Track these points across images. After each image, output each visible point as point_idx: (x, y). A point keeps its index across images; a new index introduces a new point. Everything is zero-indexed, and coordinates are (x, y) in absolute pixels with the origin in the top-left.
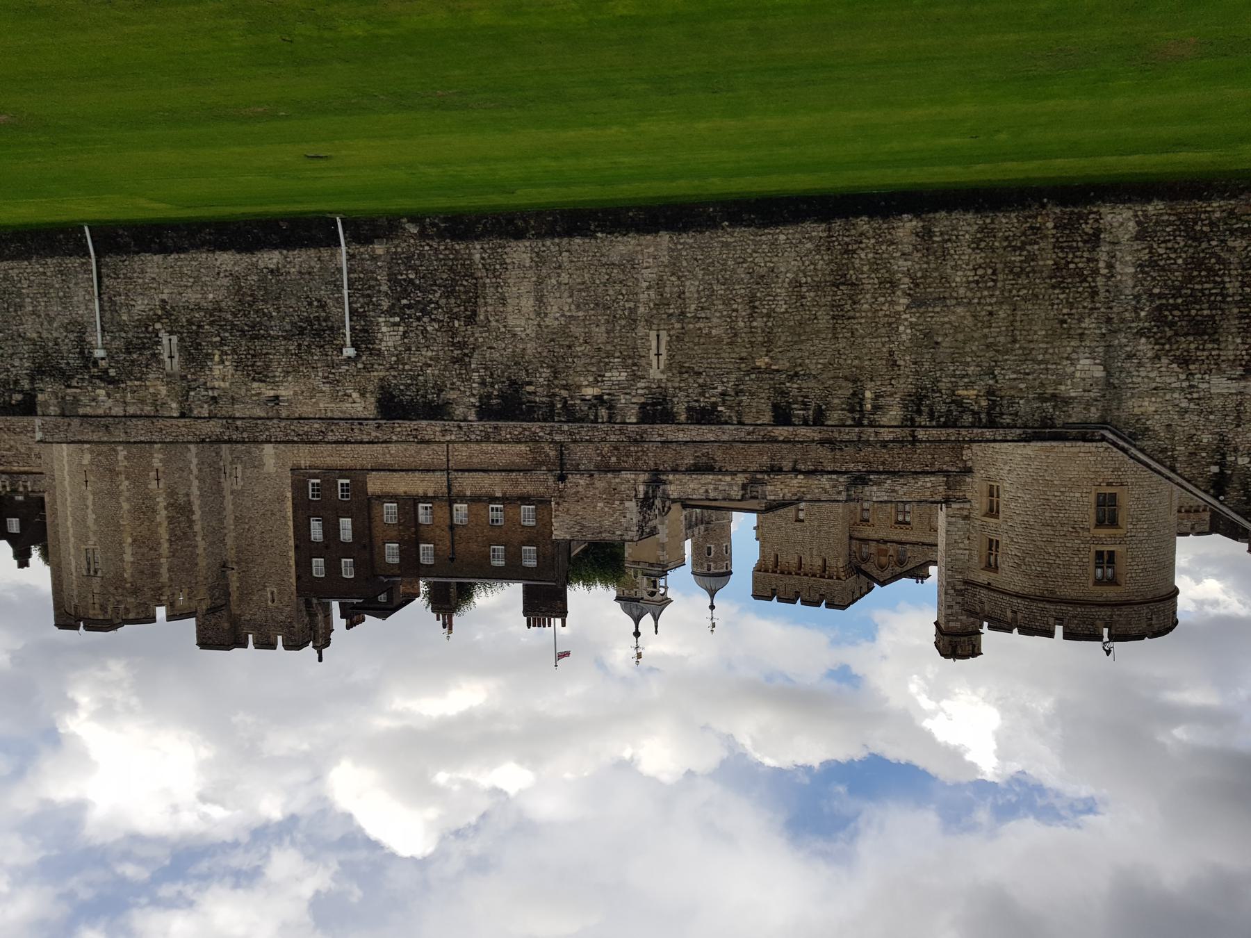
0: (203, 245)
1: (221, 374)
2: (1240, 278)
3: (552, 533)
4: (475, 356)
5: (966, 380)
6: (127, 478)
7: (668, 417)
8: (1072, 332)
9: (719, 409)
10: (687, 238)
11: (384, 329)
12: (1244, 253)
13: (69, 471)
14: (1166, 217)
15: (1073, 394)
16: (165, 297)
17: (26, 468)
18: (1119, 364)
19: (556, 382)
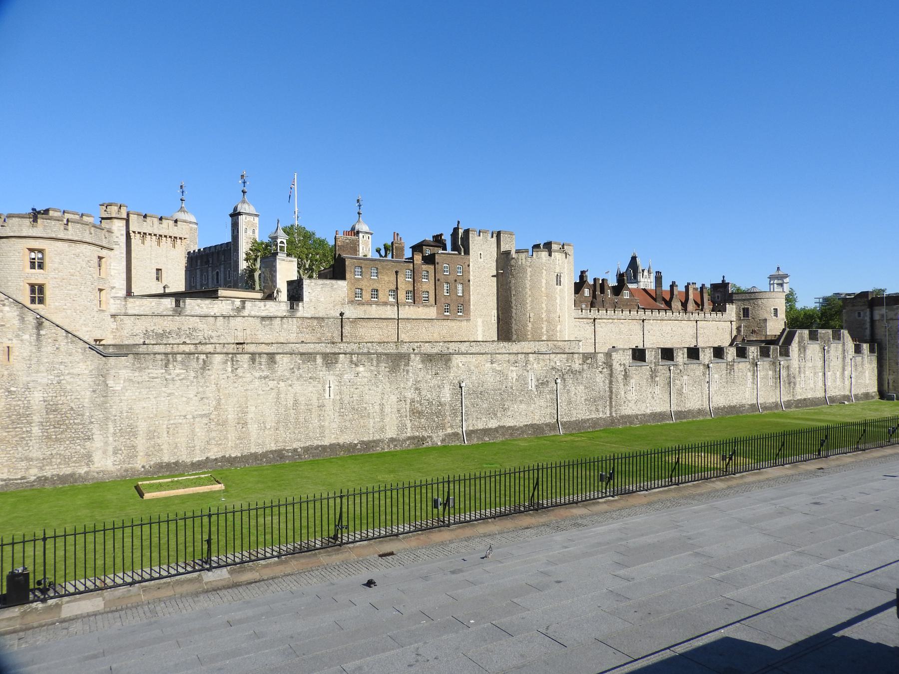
0: (517, 429)
1: (513, 374)
2: (33, 435)
3: (347, 285)
4: (410, 384)
5: (180, 378)
6: (543, 318)
7: (325, 356)
8: (126, 404)
9: (301, 361)
10: (316, 443)
11: (448, 395)
12: (31, 448)
13: (565, 322)
14: (77, 465)
15: (124, 371)
16: (533, 405)
17: (581, 320)
18: (100, 387)
19: (376, 373)
